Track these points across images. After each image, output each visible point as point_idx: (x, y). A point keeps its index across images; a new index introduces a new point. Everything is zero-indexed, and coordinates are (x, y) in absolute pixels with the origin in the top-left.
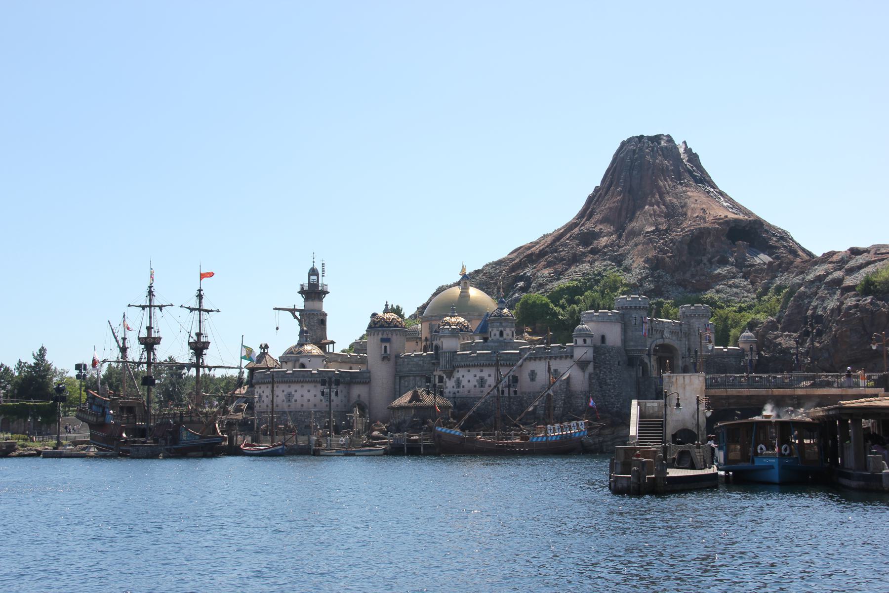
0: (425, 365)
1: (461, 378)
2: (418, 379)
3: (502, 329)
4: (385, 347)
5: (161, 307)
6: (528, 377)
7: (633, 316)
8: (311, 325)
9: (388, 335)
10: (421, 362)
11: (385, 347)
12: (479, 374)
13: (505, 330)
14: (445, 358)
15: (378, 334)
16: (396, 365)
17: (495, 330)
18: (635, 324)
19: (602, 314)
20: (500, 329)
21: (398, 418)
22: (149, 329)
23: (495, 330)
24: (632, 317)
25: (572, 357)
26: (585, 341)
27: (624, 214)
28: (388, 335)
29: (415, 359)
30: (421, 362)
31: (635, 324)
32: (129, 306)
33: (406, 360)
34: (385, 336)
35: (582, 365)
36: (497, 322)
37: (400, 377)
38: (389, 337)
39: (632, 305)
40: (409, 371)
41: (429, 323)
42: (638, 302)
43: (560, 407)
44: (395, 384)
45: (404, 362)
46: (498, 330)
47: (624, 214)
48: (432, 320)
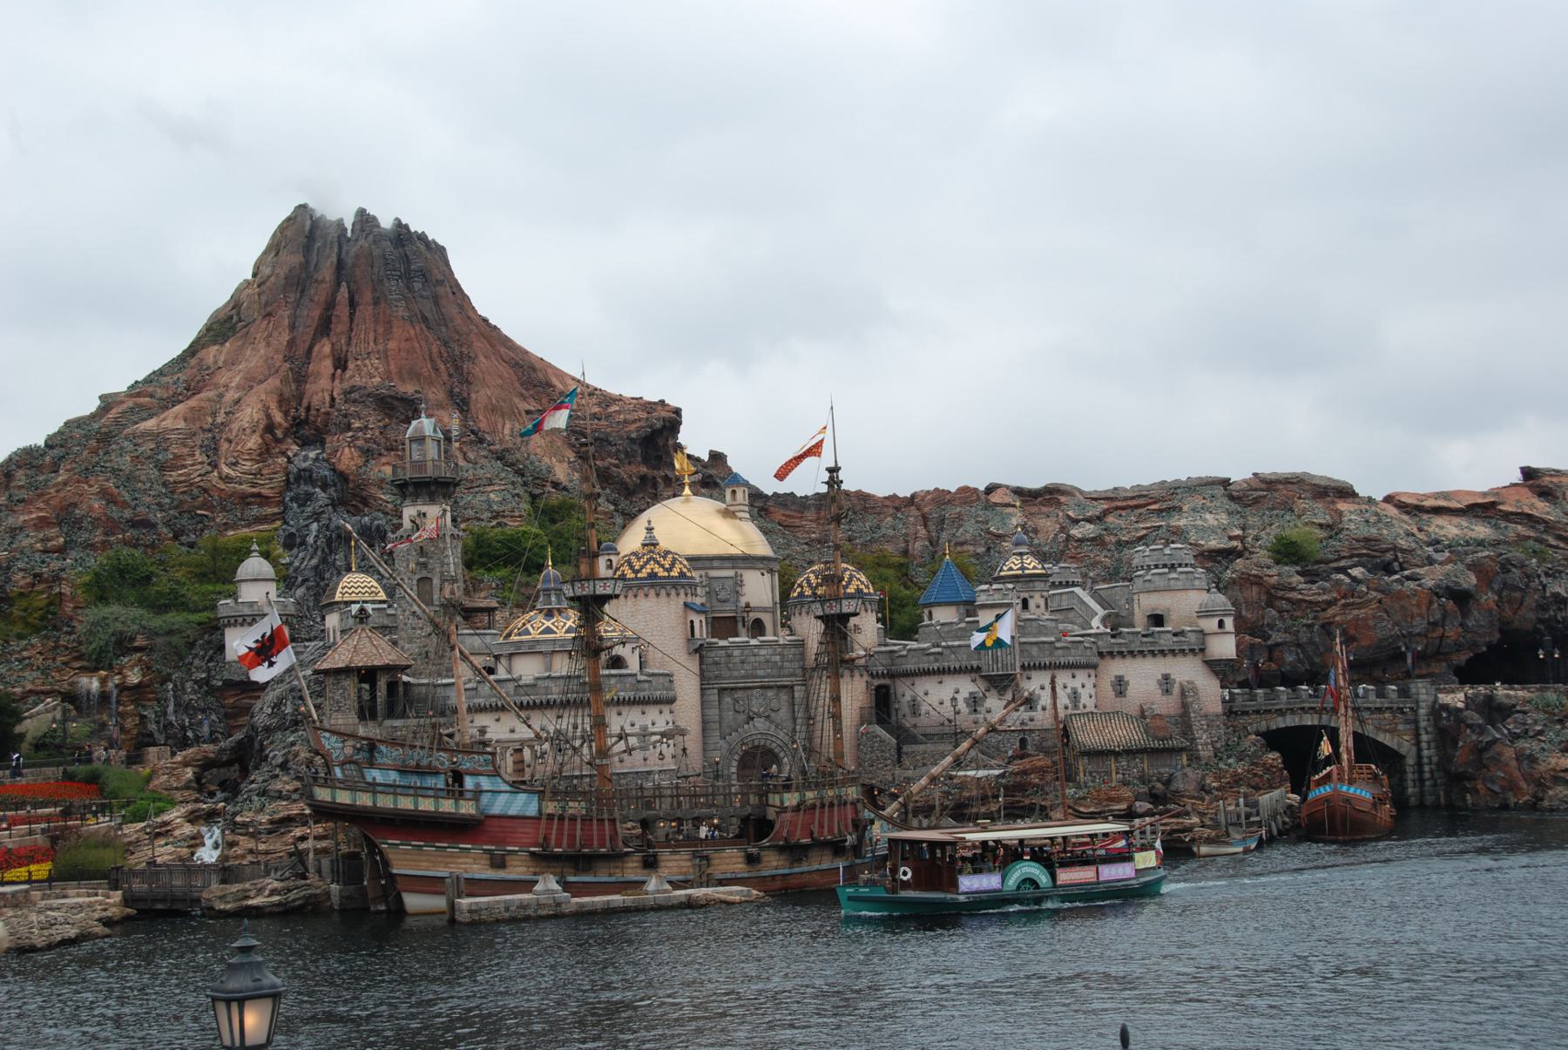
0: (786, 664)
1: (1080, 690)
2: (770, 693)
6: (1110, 688)
10: (778, 658)
12: (1071, 683)
15: (678, 595)
17: (1037, 596)
21: (1117, 773)
23: (1037, 596)
25: (1202, 650)
27: (442, 367)
29: (763, 652)
30: (778, 658)
33: (736, 653)
35: (1218, 668)
37: (722, 691)
40: (743, 677)
41: (703, 573)
43: (1207, 744)
44: (704, 703)
45: (729, 656)
47: (442, 367)
48: (712, 568)
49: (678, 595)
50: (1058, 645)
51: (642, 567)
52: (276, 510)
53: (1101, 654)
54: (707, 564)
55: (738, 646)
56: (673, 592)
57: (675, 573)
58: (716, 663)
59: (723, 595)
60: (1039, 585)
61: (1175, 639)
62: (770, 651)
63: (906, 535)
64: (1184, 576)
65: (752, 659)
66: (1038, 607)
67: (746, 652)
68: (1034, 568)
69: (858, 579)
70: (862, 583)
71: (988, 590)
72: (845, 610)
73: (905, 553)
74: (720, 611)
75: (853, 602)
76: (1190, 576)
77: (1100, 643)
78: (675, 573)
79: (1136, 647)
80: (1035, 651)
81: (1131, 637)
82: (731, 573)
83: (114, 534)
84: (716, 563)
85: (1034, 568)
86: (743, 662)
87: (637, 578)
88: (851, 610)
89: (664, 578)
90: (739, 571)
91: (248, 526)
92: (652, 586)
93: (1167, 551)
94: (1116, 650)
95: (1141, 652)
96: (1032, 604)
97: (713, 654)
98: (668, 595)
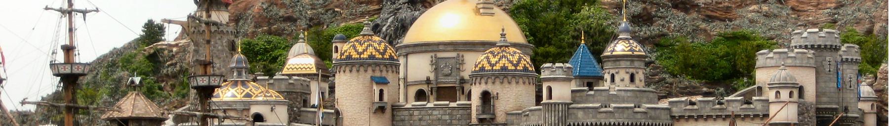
3: (634, 71)
4: (381, 92)
5: (84, 13)
7: (828, 59)
8: (218, 51)
9: (381, 71)
10: (447, 117)
11: (381, 92)
13: (637, 73)
14: (557, 113)
15: (366, 71)
16: (393, 120)
18: (830, 71)
19: (800, 55)
20: (631, 71)
22: (68, 50)
24: (825, 60)
25: (766, 116)
26: (791, 94)
28: (381, 71)
29: (435, 113)
31: (830, 71)
32: (47, 8)
33: (416, 113)
34: (378, 74)
36: (627, 60)
38: (383, 76)
39: (827, 44)
41: (433, 54)
42: (833, 39)
46: (627, 73)
48: (439, 51)
49: (366, 71)
50: (637, 109)
51: (364, 51)
52: (377, 7)
53: (673, 117)
54: (435, 48)
55: (415, 108)
56: (390, 69)
57: (387, 56)
58: (403, 120)
59: (447, 71)
60: (623, 64)
61: (745, 106)
62: (441, 112)
63: (874, 17)
64: (777, 56)
65: (427, 117)
66: (622, 80)
67: (423, 113)
68: (639, 51)
69: (525, 60)
70: (528, 63)
71: (551, 67)
72: (213, 83)
73: (869, 32)
74: (444, 83)
75: (218, 79)
76: (783, 56)
77: (674, 109)
78: (387, 56)
79: (705, 113)
80: (580, 114)
81: (702, 105)
82: (453, 54)
83: (261, 26)
84: (441, 48)
85: (639, 51)
86: (420, 120)
87: (360, 59)
88: (216, 83)
89: (379, 59)
90: (461, 53)
91: (353, 19)
92: (347, 65)
93: (822, 34)
94: (687, 114)
95: (711, 116)
96: (617, 78)
97: (400, 113)
98: (393, 72)
